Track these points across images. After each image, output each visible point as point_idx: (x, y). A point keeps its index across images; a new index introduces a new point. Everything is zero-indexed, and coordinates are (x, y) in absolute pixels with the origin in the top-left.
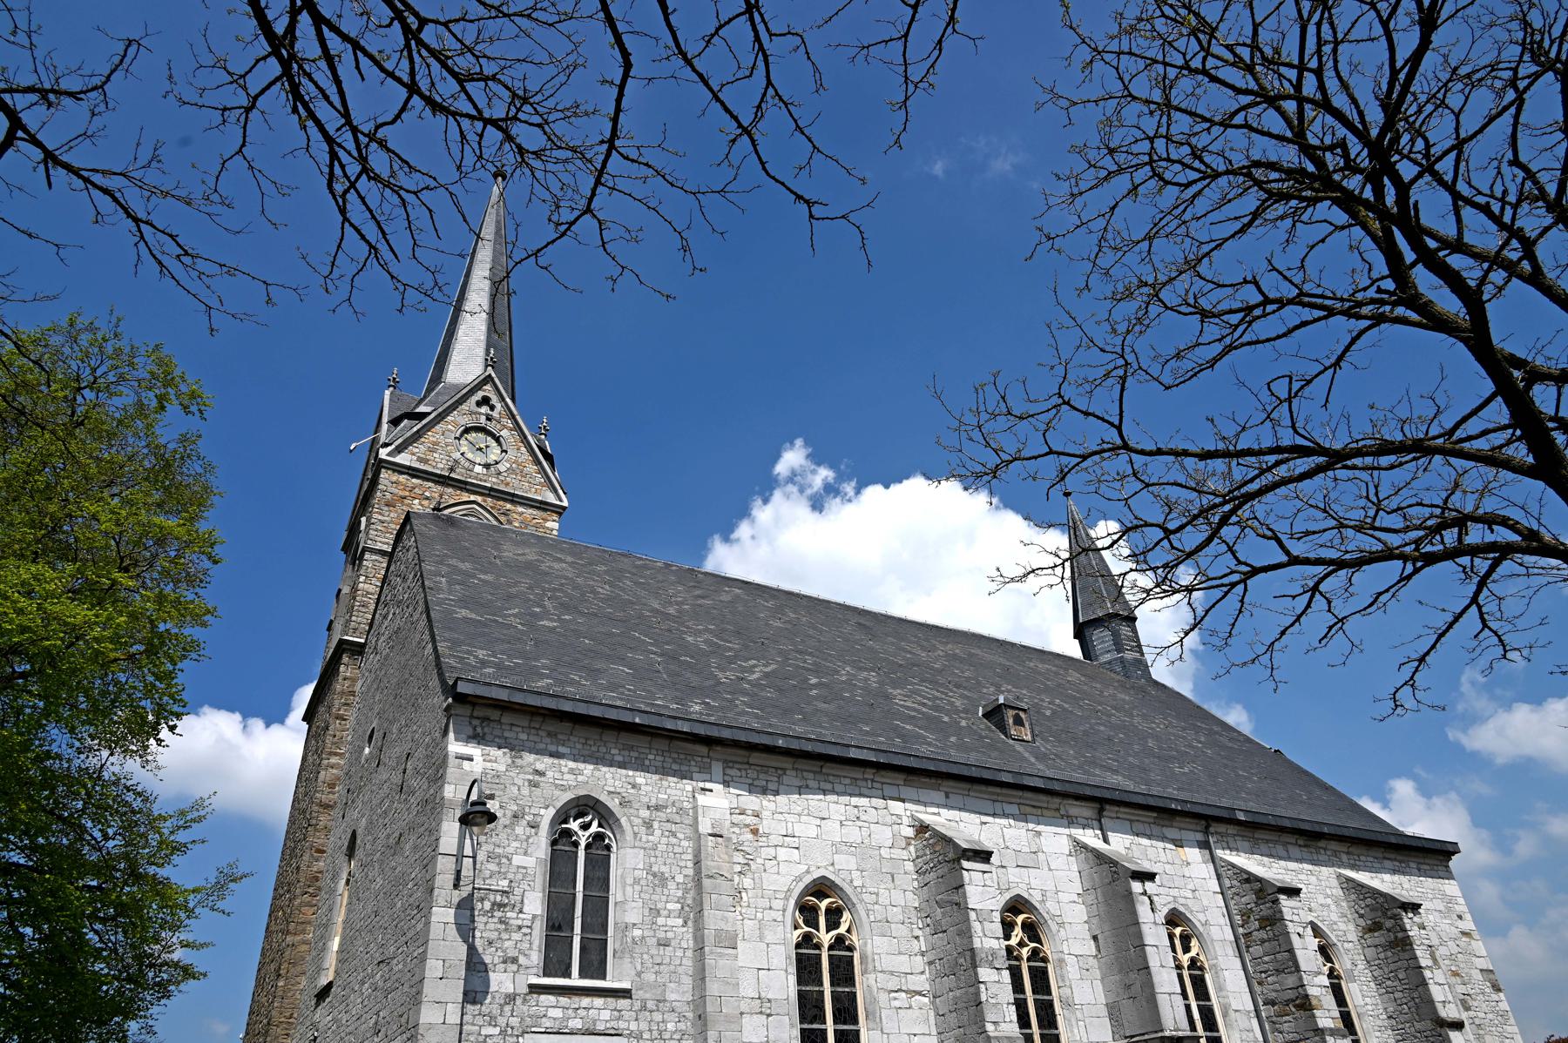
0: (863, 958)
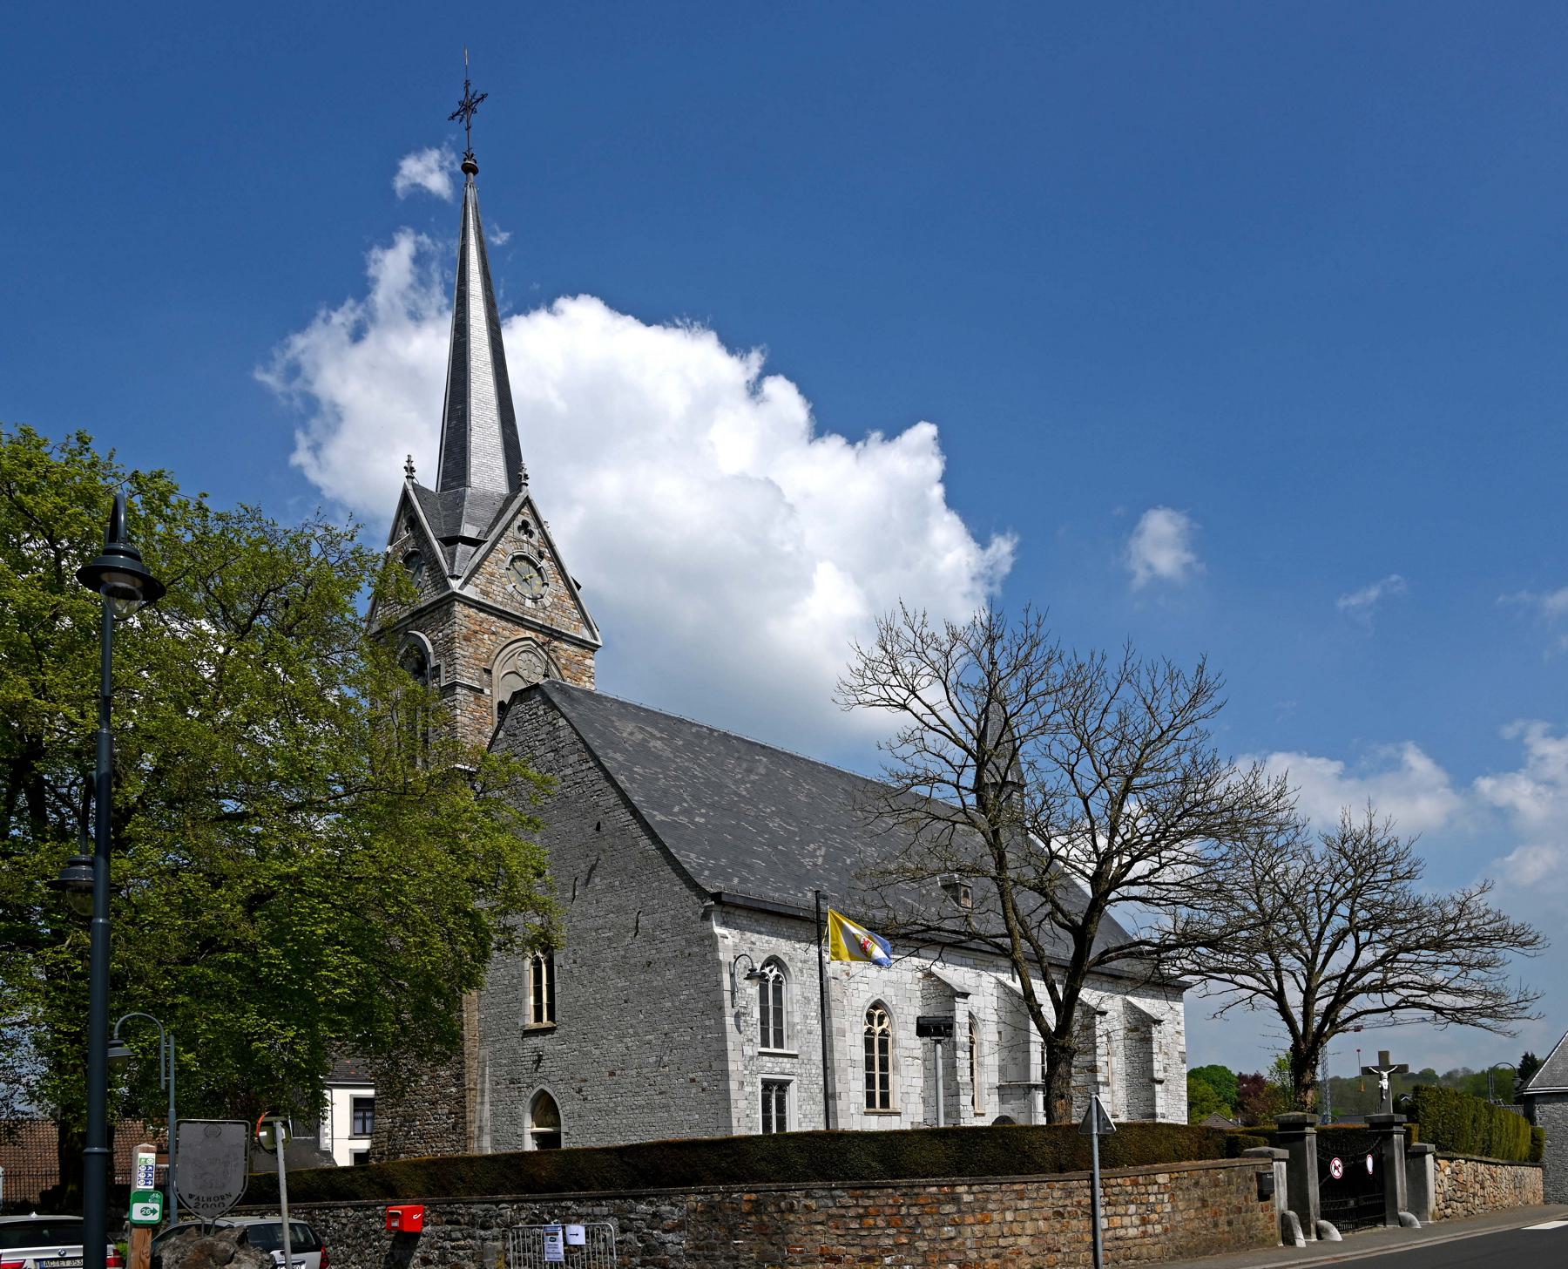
0: (894, 1041)
